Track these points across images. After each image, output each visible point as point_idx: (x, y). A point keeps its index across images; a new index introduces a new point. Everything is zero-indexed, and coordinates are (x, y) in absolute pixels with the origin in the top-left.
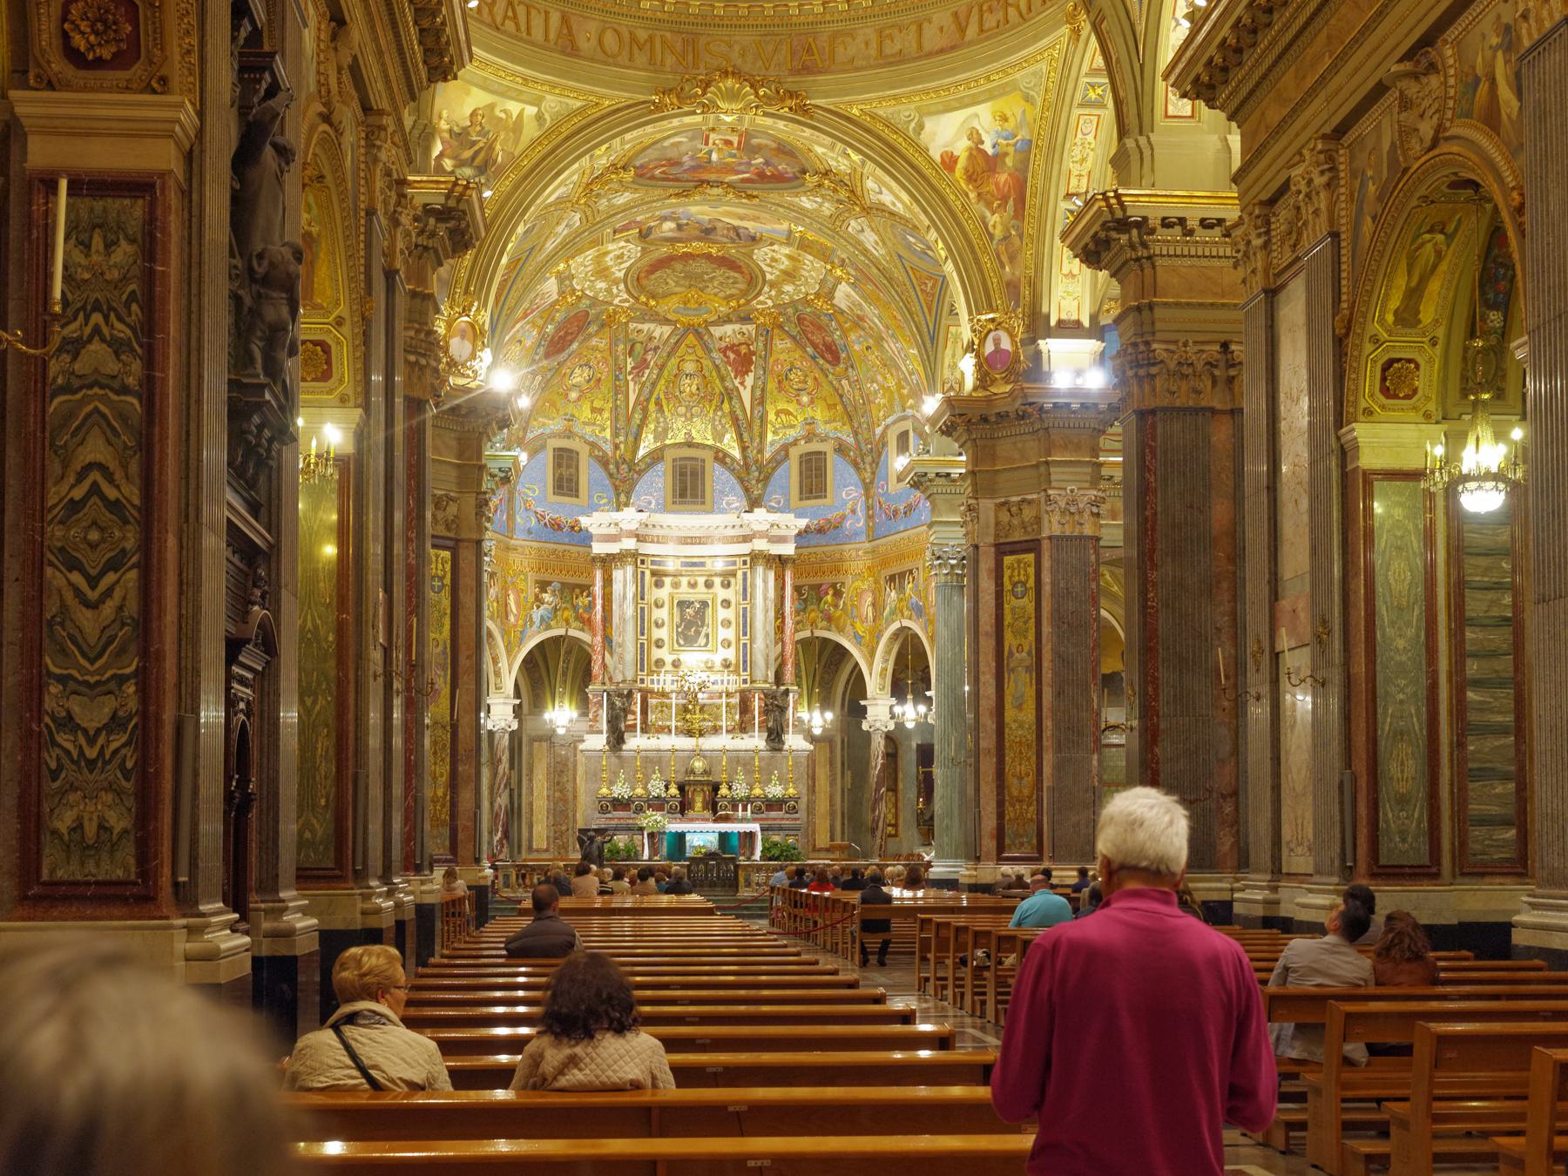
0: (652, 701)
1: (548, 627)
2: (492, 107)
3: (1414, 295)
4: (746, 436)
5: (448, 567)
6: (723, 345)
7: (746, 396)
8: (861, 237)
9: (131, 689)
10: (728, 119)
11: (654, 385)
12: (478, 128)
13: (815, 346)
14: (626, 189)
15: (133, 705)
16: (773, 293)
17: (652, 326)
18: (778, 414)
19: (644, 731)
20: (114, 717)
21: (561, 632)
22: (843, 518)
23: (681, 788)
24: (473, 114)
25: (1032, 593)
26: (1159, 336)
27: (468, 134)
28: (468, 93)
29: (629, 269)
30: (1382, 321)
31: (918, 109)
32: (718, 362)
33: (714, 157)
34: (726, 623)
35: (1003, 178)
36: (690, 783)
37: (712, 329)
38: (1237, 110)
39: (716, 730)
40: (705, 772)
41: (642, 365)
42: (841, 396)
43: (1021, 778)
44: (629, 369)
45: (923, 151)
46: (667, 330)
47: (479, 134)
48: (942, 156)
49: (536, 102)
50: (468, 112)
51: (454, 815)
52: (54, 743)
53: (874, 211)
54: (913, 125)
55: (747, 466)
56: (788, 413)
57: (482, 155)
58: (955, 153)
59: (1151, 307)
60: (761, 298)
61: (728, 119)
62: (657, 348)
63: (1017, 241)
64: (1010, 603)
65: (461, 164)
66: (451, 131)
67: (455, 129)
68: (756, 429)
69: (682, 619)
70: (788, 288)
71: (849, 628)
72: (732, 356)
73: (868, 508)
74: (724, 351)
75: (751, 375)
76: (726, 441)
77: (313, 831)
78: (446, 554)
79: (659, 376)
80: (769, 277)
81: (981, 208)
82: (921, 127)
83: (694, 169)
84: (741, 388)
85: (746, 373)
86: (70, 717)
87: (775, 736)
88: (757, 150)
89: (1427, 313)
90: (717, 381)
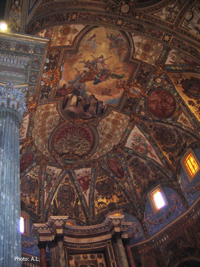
6: (79, 177)
7: (87, 198)
11: (54, 194)
16: (100, 151)
29: (52, 133)
32: (77, 185)
37: (75, 171)
42: (124, 190)
44: (45, 186)
46: (60, 170)
56: (102, 203)
60: (95, 154)
62: (55, 179)
68: (91, 211)
70: (107, 146)
72: (82, 182)
73: (143, 228)
74: (79, 180)
75: (89, 189)
76: (80, 217)
79: (55, 190)
80: (101, 141)
84: (85, 195)
90: (76, 194)
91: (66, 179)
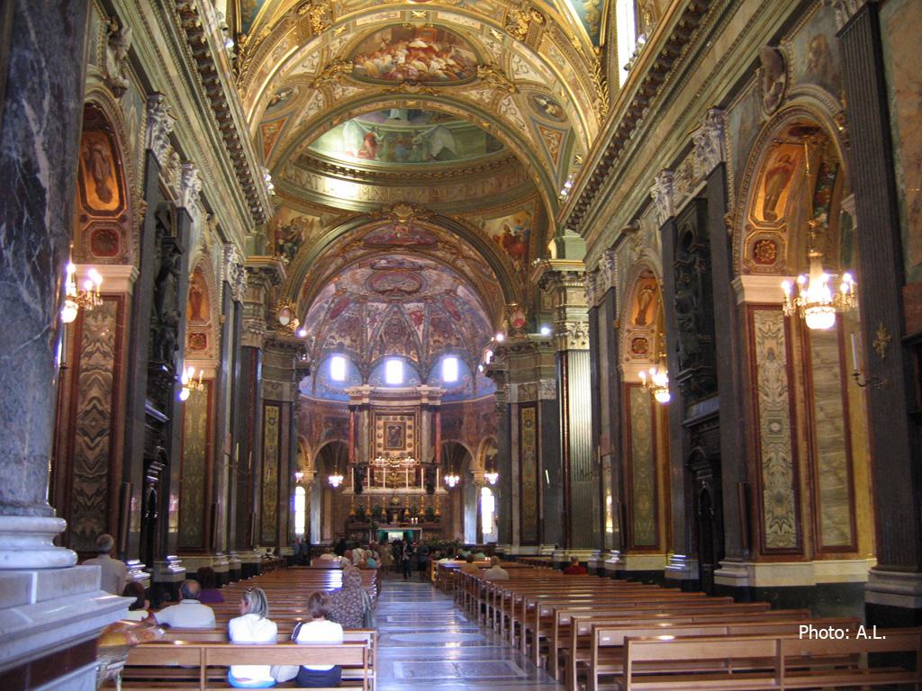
0: (376, 471)
1: (330, 437)
2: (300, 218)
3: (643, 313)
4: (420, 353)
5: (277, 414)
7: (420, 334)
8: (464, 269)
9: (104, 480)
10: (402, 221)
13: (450, 312)
14: (361, 249)
15: (105, 486)
17: (378, 304)
18: (435, 342)
19: (373, 484)
20: (98, 489)
21: (336, 440)
22: (463, 388)
23: (387, 511)
24: (292, 221)
25: (534, 425)
26: (568, 320)
30: (630, 323)
33: (398, 235)
34: (410, 436)
35: (519, 246)
36: (392, 509)
38: (585, 233)
39: (404, 485)
40: (398, 504)
41: (373, 321)
43: (530, 508)
45: (485, 235)
46: (385, 305)
47: (295, 229)
49: (320, 215)
51: (278, 524)
52: (76, 499)
53: (466, 258)
55: (421, 366)
56: (438, 341)
57: (296, 237)
59: (564, 308)
61: (402, 221)
62: (380, 314)
63: (525, 272)
64: (525, 429)
65: (286, 241)
66: (282, 228)
69: (390, 434)
70: (437, 287)
71: (466, 439)
72: (414, 317)
74: (410, 314)
77: (194, 532)
78: (277, 408)
81: (509, 259)
82: (484, 225)
83: (389, 240)
85: (421, 323)
86: (82, 490)
87: (430, 488)
88: (417, 233)
89: (649, 319)
91: (394, 312)
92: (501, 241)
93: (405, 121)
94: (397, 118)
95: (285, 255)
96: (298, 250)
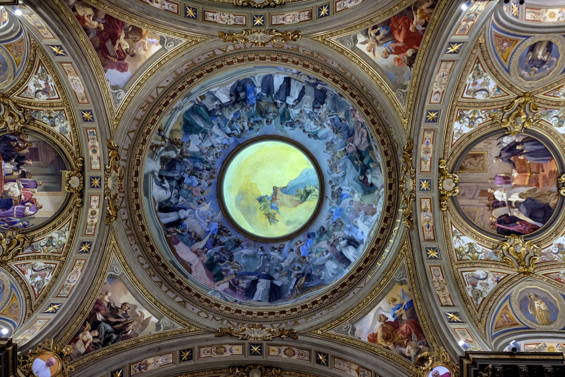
2: (135, 307)
12: (124, 312)
24: (124, 304)
27: (118, 312)
28: (126, 293)
31: (350, 322)
35: (404, 327)
47: (123, 315)
48: (368, 338)
50: (122, 302)
54: (350, 331)
57: (120, 325)
58: (375, 332)
65: (108, 322)
66: (109, 304)
67: (112, 304)
82: (354, 330)
92: (380, 340)
93: (267, 303)
94: (259, 301)
95: (96, 333)
96: (115, 341)
